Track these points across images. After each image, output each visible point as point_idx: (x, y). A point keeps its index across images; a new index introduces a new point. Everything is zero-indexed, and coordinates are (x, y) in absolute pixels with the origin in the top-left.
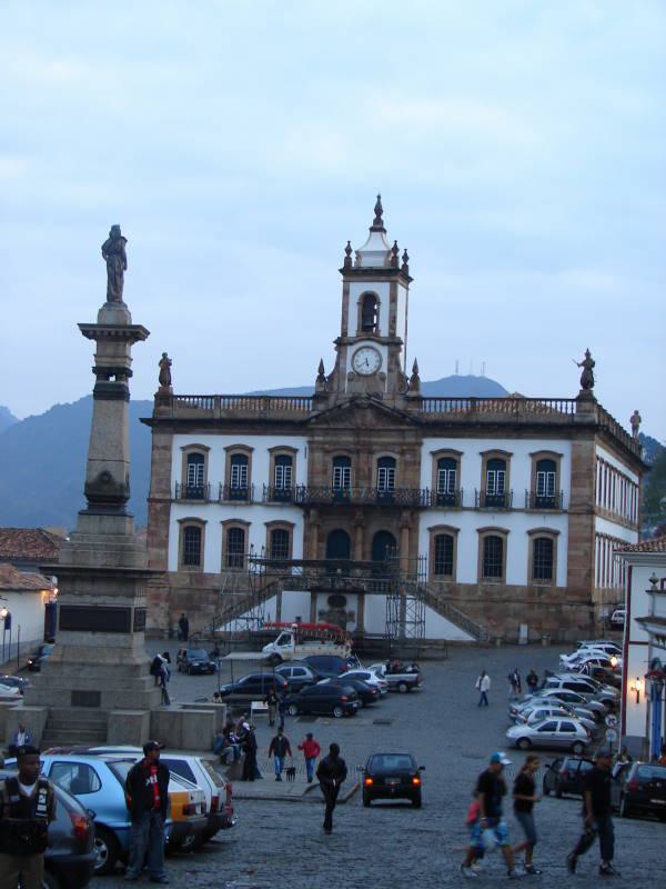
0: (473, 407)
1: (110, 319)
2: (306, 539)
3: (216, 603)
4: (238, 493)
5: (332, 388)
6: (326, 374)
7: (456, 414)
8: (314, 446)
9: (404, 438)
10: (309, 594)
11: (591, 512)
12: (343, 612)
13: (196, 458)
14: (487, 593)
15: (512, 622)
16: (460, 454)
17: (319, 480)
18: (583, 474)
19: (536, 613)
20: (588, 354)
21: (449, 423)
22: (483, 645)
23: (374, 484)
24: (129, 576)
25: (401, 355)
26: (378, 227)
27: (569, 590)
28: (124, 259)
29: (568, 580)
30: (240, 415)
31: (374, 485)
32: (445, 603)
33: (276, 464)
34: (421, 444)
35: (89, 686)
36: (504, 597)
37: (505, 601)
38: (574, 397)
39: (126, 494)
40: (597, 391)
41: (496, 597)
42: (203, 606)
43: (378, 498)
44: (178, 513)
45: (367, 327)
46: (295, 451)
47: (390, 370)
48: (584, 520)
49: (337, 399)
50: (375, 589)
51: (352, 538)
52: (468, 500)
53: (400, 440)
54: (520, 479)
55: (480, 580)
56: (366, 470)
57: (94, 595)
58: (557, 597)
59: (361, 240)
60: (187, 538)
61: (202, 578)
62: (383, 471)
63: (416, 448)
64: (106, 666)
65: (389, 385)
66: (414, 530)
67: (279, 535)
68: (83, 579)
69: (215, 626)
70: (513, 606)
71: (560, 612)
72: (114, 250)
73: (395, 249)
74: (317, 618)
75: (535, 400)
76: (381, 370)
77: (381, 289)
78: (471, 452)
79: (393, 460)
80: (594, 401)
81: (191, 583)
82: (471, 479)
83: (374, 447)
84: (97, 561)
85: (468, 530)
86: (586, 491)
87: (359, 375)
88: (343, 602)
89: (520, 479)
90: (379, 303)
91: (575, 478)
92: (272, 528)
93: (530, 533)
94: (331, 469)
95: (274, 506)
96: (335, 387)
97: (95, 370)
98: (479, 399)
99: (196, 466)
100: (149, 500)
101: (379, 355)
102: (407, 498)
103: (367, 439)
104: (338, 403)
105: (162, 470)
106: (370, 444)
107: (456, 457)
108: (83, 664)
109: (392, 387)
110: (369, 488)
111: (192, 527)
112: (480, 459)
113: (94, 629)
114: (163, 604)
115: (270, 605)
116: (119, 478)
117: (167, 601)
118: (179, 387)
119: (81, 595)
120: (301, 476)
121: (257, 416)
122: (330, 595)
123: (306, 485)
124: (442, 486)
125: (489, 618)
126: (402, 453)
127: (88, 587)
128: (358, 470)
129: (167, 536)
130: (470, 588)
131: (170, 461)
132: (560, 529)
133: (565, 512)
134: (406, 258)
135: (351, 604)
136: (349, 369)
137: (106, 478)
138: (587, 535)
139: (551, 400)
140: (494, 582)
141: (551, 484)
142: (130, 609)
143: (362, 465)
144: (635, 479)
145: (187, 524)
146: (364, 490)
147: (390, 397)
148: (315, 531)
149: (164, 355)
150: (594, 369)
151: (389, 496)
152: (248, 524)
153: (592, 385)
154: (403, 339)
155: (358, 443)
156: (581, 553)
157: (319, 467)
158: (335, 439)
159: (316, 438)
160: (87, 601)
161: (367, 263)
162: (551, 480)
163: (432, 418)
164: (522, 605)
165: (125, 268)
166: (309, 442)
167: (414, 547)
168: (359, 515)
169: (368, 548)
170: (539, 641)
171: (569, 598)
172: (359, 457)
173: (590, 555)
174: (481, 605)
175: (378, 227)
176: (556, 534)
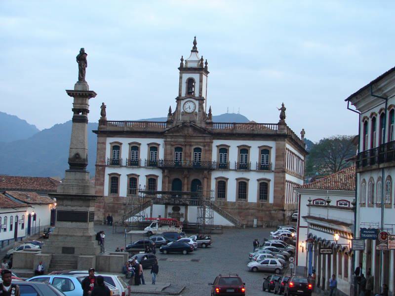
0: (235, 127)
1: (80, 88)
3: (124, 209)
4: (134, 162)
5: (174, 118)
6: (172, 112)
7: (227, 130)
8: (167, 143)
9: (205, 139)
10: (164, 206)
11: (284, 172)
12: (179, 213)
13: (116, 148)
15: (250, 218)
16: (229, 147)
17: (169, 157)
18: (280, 155)
19: (261, 214)
20: (283, 105)
22: (238, 228)
23: (192, 159)
24: (87, 198)
25: (204, 104)
26: (194, 50)
27: (275, 204)
28: (86, 63)
30: (135, 130)
31: (192, 160)
32: (222, 209)
34: (212, 142)
35: (69, 245)
36: (247, 207)
37: (247, 209)
39: (86, 163)
40: (286, 121)
42: (119, 211)
43: (194, 165)
44: (109, 171)
45: (190, 93)
46: (159, 145)
47: (199, 111)
48: (281, 175)
49: (177, 123)
50: (192, 204)
51: (183, 182)
52: (232, 166)
53: (204, 141)
54: (254, 157)
55: (237, 200)
57: (72, 206)
58: (269, 207)
59: (187, 55)
60: (112, 182)
61: (118, 198)
63: (211, 144)
64: (78, 236)
66: (209, 179)
67: (152, 181)
68: (67, 199)
69: (124, 219)
70: (251, 211)
71: (271, 214)
72: (82, 58)
73: (202, 60)
74: (168, 216)
75: (261, 124)
77: (196, 77)
78: (234, 146)
79: (200, 149)
80: (285, 124)
82: (233, 157)
83: (193, 144)
84: (74, 192)
85: (232, 178)
86: (282, 163)
88: (179, 209)
89: (254, 157)
90: (195, 83)
91: (277, 157)
92: (149, 178)
93: (258, 180)
94: (174, 153)
95: (150, 168)
96: (176, 118)
97: (73, 110)
98: (237, 124)
99: (116, 151)
100: (96, 165)
101: (195, 104)
102: (206, 165)
104: (178, 124)
105: (102, 153)
106: (191, 142)
107: (227, 148)
108: (67, 236)
109: (200, 118)
110: (190, 161)
111: (114, 177)
112: (237, 149)
113: (72, 221)
114: (101, 210)
115: (147, 211)
116: (83, 156)
117: (103, 208)
118: (109, 117)
119: (66, 206)
120: (161, 156)
121: (142, 130)
122: (172, 206)
123: (163, 159)
124: (221, 160)
125: (240, 217)
126: (204, 146)
127: (69, 203)
128: (185, 153)
129: (104, 181)
130: (233, 204)
131: (105, 149)
132: (271, 179)
133: (273, 171)
134: (206, 63)
135: (182, 210)
136: (182, 110)
137: (77, 156)
138: (283, 181)
139: (267, 124)
140: (243, 200)
141: (267, 160)
142: (87, 212)
143: (187, 151)
144: (302, 158)
145: (112, 176)
146: (188, 162)
147: (199, 122)
148: (167, 179)
149: (103, 103)
150: (285, 111)
151: (198, 164)
153: (285, 118)
154: (205, 98)
155: (185, 142)
157: (169, 152)
158: (176, 140)
159: (168, 140)
160: (69, 208)
161: (190, 65)
162: (267, 158)
163: (217, 131)
165: (86, 66)
166: (165, 141)
167: (209, 186)
168: (186, 172)
169: (190, 186)
170: (262, 226)
171: (274, 208)
173: (283, 189)
174: (237, 210)
175: (194, 50)
176: (269, 181)
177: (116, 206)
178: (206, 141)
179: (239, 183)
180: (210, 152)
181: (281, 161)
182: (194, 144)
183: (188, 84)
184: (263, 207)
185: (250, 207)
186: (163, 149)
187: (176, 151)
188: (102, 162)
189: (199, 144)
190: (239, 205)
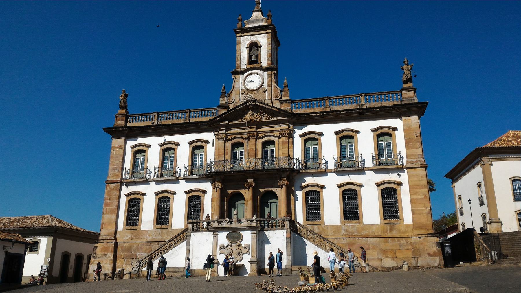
2: (213, 201)
5: (231, 100)
14: (349, 232)
19: (390, 245)
21: (311, 113)
29: (413, 219)
36: (364, 233)
41: (356, 234)
46: (207, 142)
47: (269, 86)
53: (278, 128)
56: (255, 149)
58: (405, 232)
61: (141, 233)
79: (273, 143)
81: (132, 238)
87: (249, 90)
88: (240, 238)
91: (408, 143)
93: (378, 185)
102: (285, 165)
106: (258, 133)
107: (317, 137)
126: (279, 137)
136: (241, 87)
159: (220, 132)
164: (378, 239)
171: (417, 232)
177: (135, 246)
179: (344, 192)
182: (263, 134)
184: (394, 232)
188: (117, 175)
190: (346, 230)
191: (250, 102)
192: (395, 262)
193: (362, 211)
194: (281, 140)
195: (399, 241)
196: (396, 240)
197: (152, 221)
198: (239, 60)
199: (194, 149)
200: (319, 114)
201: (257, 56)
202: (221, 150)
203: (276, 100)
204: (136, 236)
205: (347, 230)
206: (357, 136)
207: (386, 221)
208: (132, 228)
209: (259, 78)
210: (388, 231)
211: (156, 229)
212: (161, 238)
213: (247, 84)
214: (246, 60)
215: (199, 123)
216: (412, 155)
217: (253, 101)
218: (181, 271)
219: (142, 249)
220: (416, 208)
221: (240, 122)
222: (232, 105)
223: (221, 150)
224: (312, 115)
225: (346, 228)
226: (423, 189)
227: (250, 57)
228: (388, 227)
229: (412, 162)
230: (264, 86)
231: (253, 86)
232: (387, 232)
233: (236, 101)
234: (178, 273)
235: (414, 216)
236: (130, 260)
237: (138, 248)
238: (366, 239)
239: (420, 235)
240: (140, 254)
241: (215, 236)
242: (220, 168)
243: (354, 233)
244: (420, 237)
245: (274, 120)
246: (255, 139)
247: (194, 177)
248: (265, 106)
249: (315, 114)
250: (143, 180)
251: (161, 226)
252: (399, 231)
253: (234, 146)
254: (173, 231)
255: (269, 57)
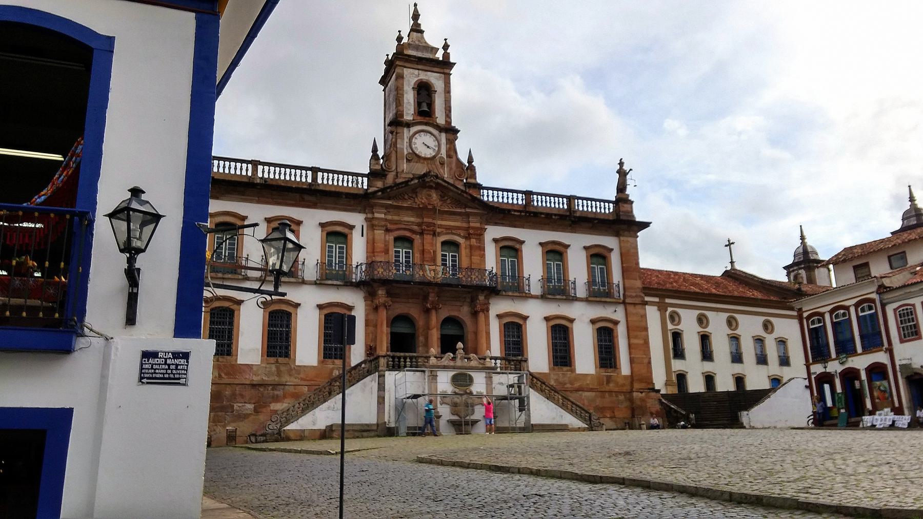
12: (471, 393)
14: (560, 383)
16: (523, 242)
19: (607, 401)
20: (621, 164)
21: (515, 211)
33: (327, 241)
36: (577, 385)
37: (578, 390)
38: (614, 199)
41: (568, 386)
42: (236, 406)
46: (352, 227)
47: (449, 156)
51: (420, 322)
53: (465, 225)
56: (432, 251)
58: (623, 385)
62: (445, 256)
65: (451, 169)
71: (631, 400)
76: (440, 155)
77: (435, 79)
81: (220, 376)
83: (438, 230)
91: (625, 271)
92: (326, 311)
103: (430, 220)
104: (399, 181)
107: (517, 246)
112: (540, 249)
122: (451, 373)
126: (468, 237)
128: (423, 252)
132: (619, 319)
133: (624, 303)
143: (427, 247)
152: (297, 305)
155: (419, 225)
156: (641, 342)
157: (380, 245)
159: (377, 215)
172: (423, 239)
176: (616, 323)
178: (472, 225)
180: (483, 252)
181: (636, 280)
183: (418, 94)
184: (611, 385)
185: (583, 384)
186: (364, 239)
187: (395, 247)
189: (458, 232)
191: (431, 178)
192: (614, 423)
193: (574, 355)
194: (468, 243)
195: (617, 396)
196: (614, 395)
197: (257, 349)
198: (402, 104)
199: (329, 234)
200: (523, 214)
201: (431, 105)
202: (379, 244)
203: (458, 179)
204: (227, 374)
205: (557, 379)
206: (566, 252)
207: (603, 370)
208: (221, 359)
209: (434, 141)
210: (605, 383)
211: (268, 364)
212: (277, 379)
213: (416, 146)
214: (413, 107)
215: (258, 185)
216: (631, 288)
217: (435, 176)
218: (373, 430)
219: (242, 396)
220: (637, 356)
221: (410, 205)
222: (392, 176)
223: (379, 244)
224: (516, 213)
225: (555, 377)
226: (643, 331)
227: (419, 104)
228: (605, 379)
229: (631, 297)
230: (442, 156)
231: (427, 153)
232: (603, 384)
233: (399, 170)
234: (368, 432)
235: (633, 365)
236: (220, 414)
237: (234, 395)
238: (580, 392)
239: (642, 389)
240: (240, 405)
241: (434, 377)
242: (391, 274)
243: (565, 384)
244: (642, 393)
245: (461, 211)
246: (432, 236)
247: (335, 282)
248: (452, 188)
249: (519, 213)
250: (240, 277)
251: (277, 360)
252: (617, 383)
253: (397, 239)
254: (299, 368)
255: (447, 112)
